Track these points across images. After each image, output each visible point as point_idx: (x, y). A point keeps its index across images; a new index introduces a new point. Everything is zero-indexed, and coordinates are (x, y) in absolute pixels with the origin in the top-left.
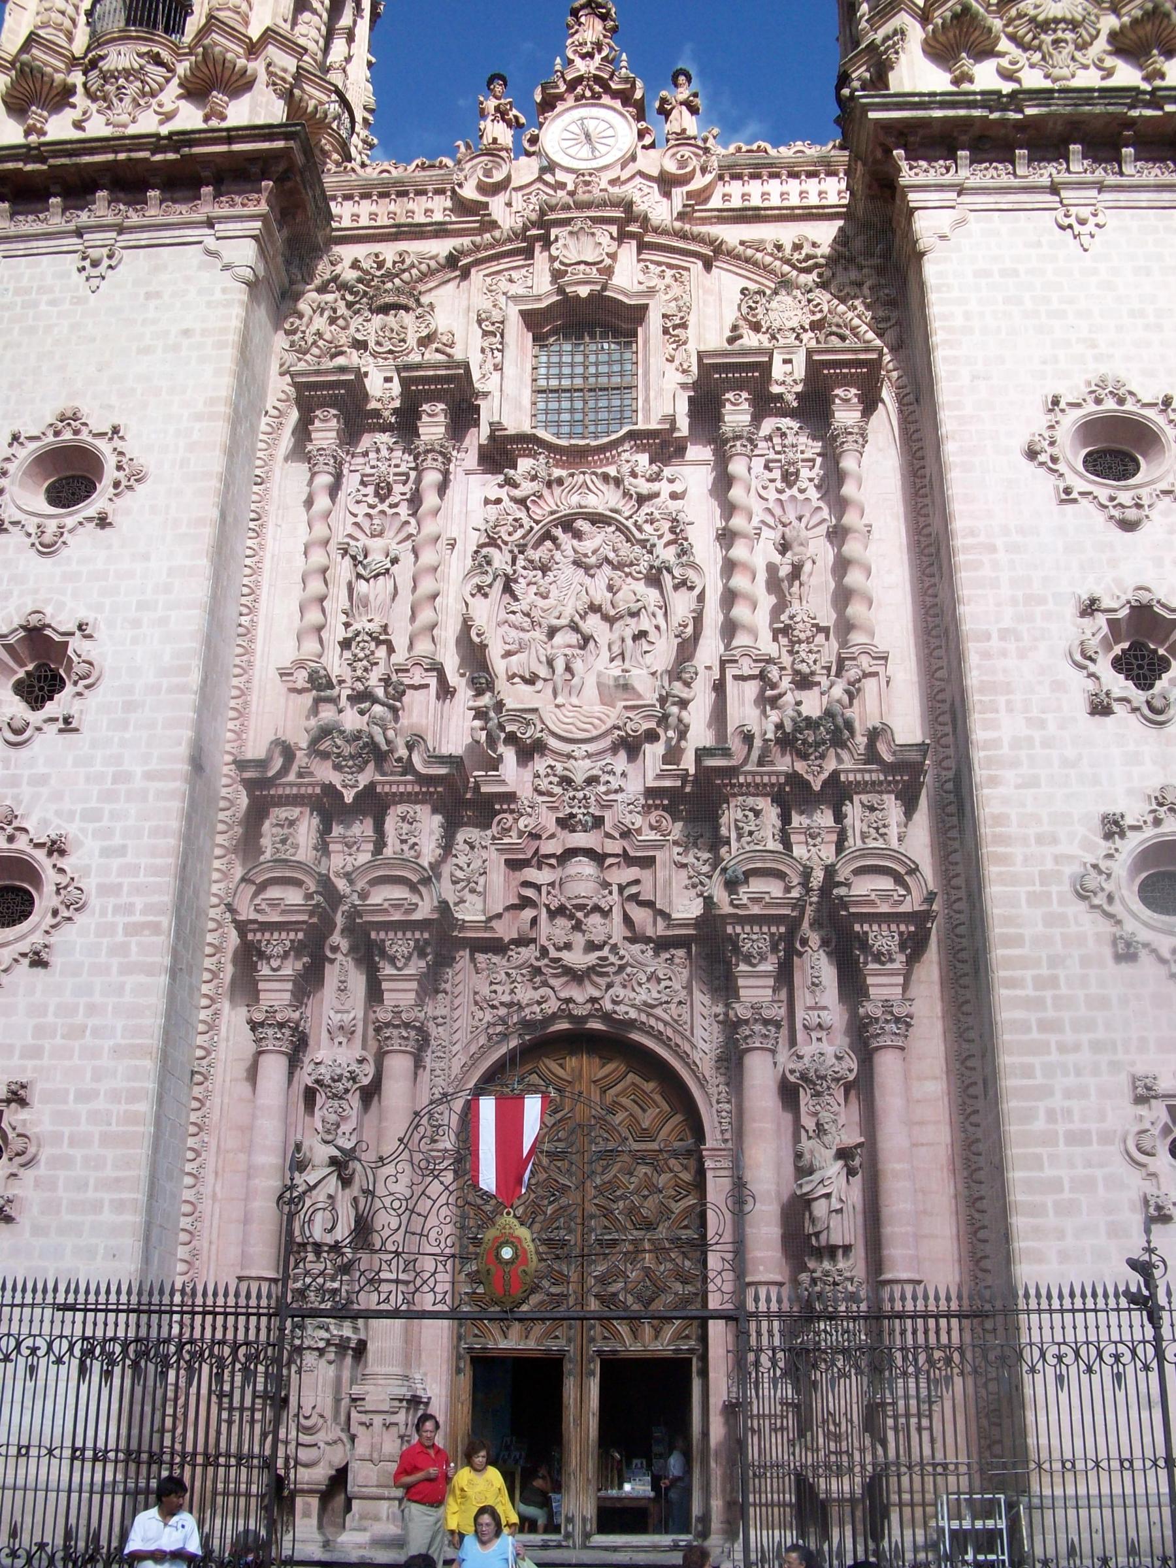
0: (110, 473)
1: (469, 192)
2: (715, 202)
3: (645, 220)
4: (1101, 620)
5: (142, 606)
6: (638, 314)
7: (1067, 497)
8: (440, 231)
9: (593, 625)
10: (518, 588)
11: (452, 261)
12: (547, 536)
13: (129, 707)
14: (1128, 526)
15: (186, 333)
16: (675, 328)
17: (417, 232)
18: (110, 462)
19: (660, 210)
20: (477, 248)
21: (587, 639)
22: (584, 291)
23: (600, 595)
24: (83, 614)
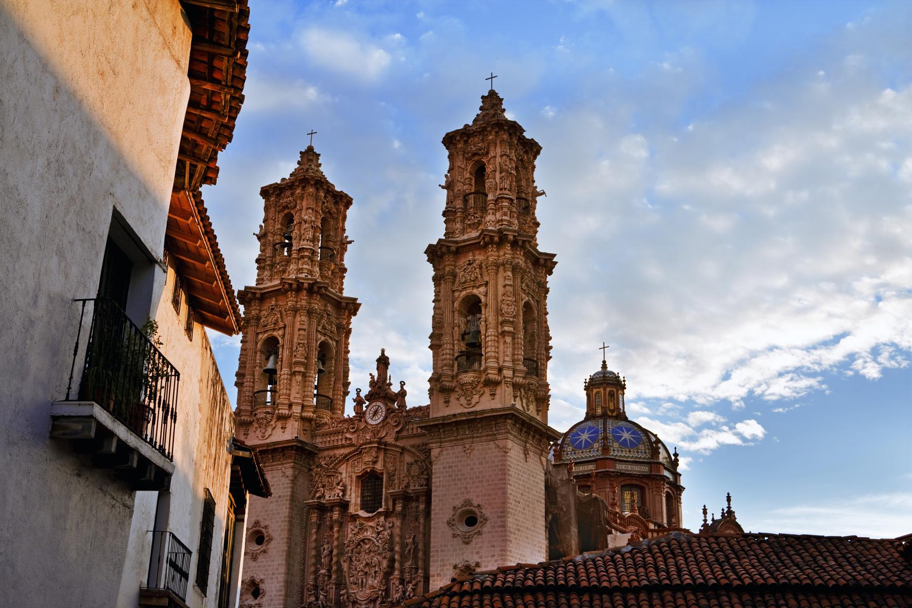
0: (266, 539)
1: (348, 436)
2: (405, 433)
3: (386, 444)
4: (458, 571)
5: (273, 574)
6: (382, 474)
7: (454, 536)
8: (343, 447)
9: (367, 570)
10: (354, 559)
11: (345, 457)
12: (359, 544)
13: (271, 600)
14: (467, 543)
15: (280, 497)
16: (391, 477)
17: (337, 447)
18: (266, 535)
19: (390, 440)
20: (350, 453)
21: (366, 573)
22: (369, 470)
23: (369, 561)
24: (262, 577)
